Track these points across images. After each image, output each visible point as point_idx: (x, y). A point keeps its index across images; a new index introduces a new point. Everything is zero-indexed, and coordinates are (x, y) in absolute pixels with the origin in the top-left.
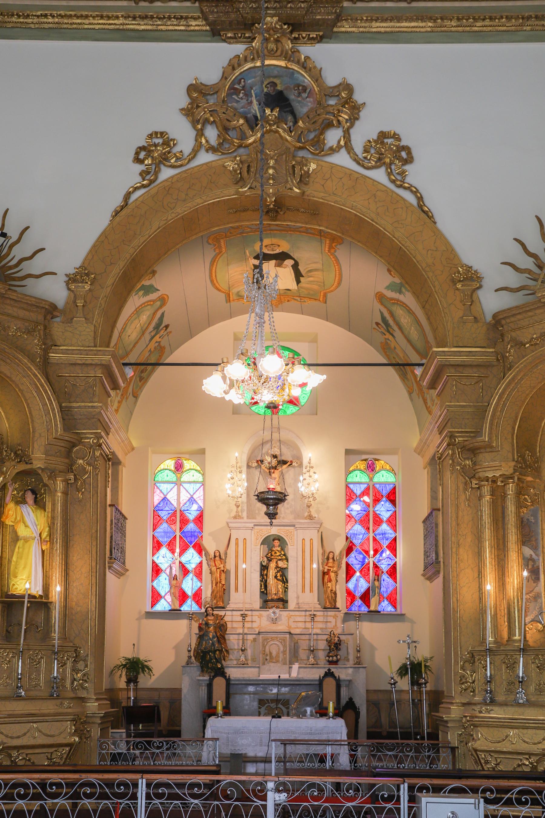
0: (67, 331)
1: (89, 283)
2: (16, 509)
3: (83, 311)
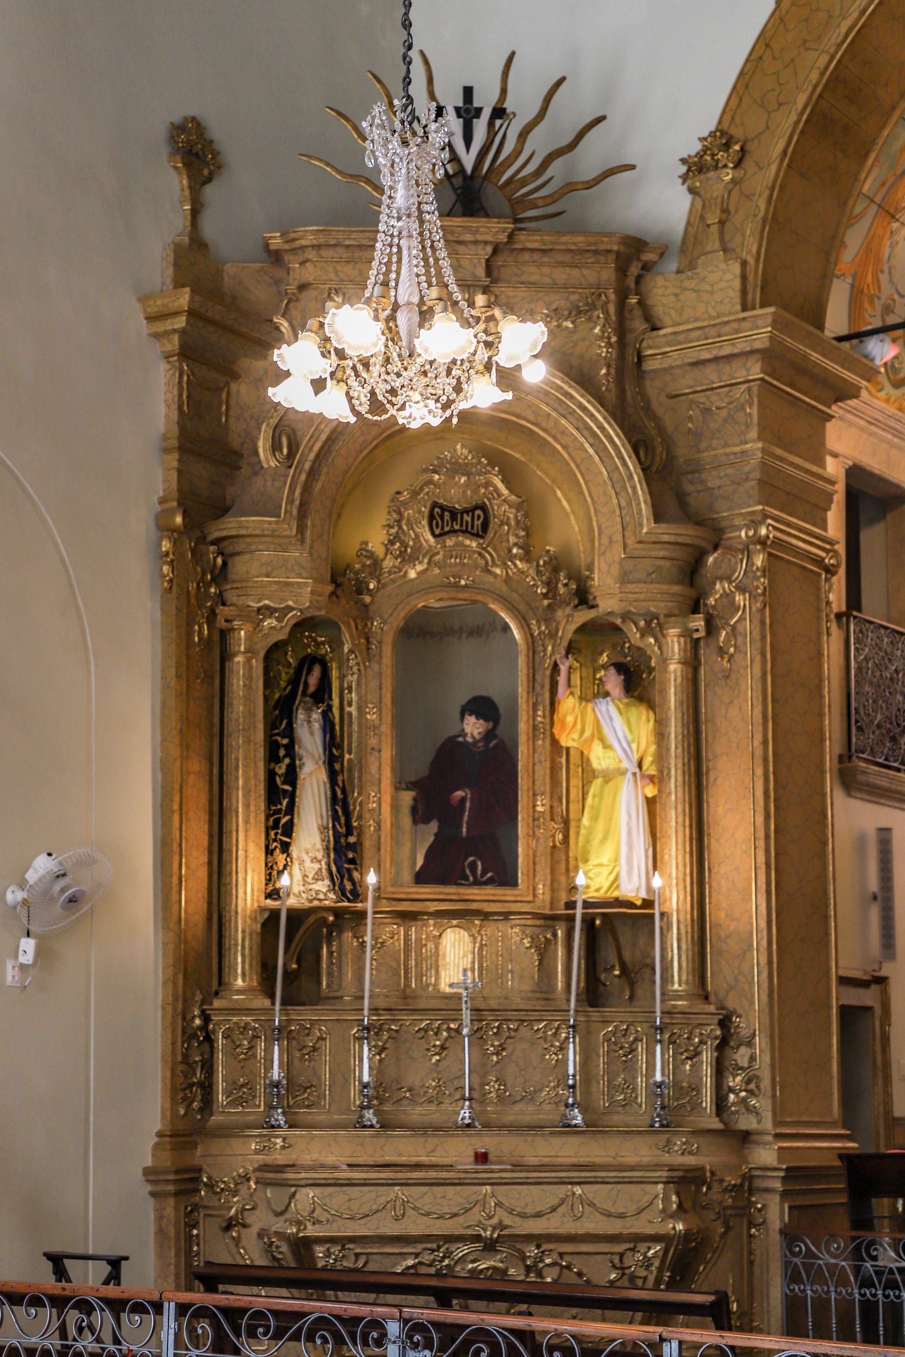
0: (686, 289)
1: (731, 165)
2: (583, 713)
3: (722, 233)
